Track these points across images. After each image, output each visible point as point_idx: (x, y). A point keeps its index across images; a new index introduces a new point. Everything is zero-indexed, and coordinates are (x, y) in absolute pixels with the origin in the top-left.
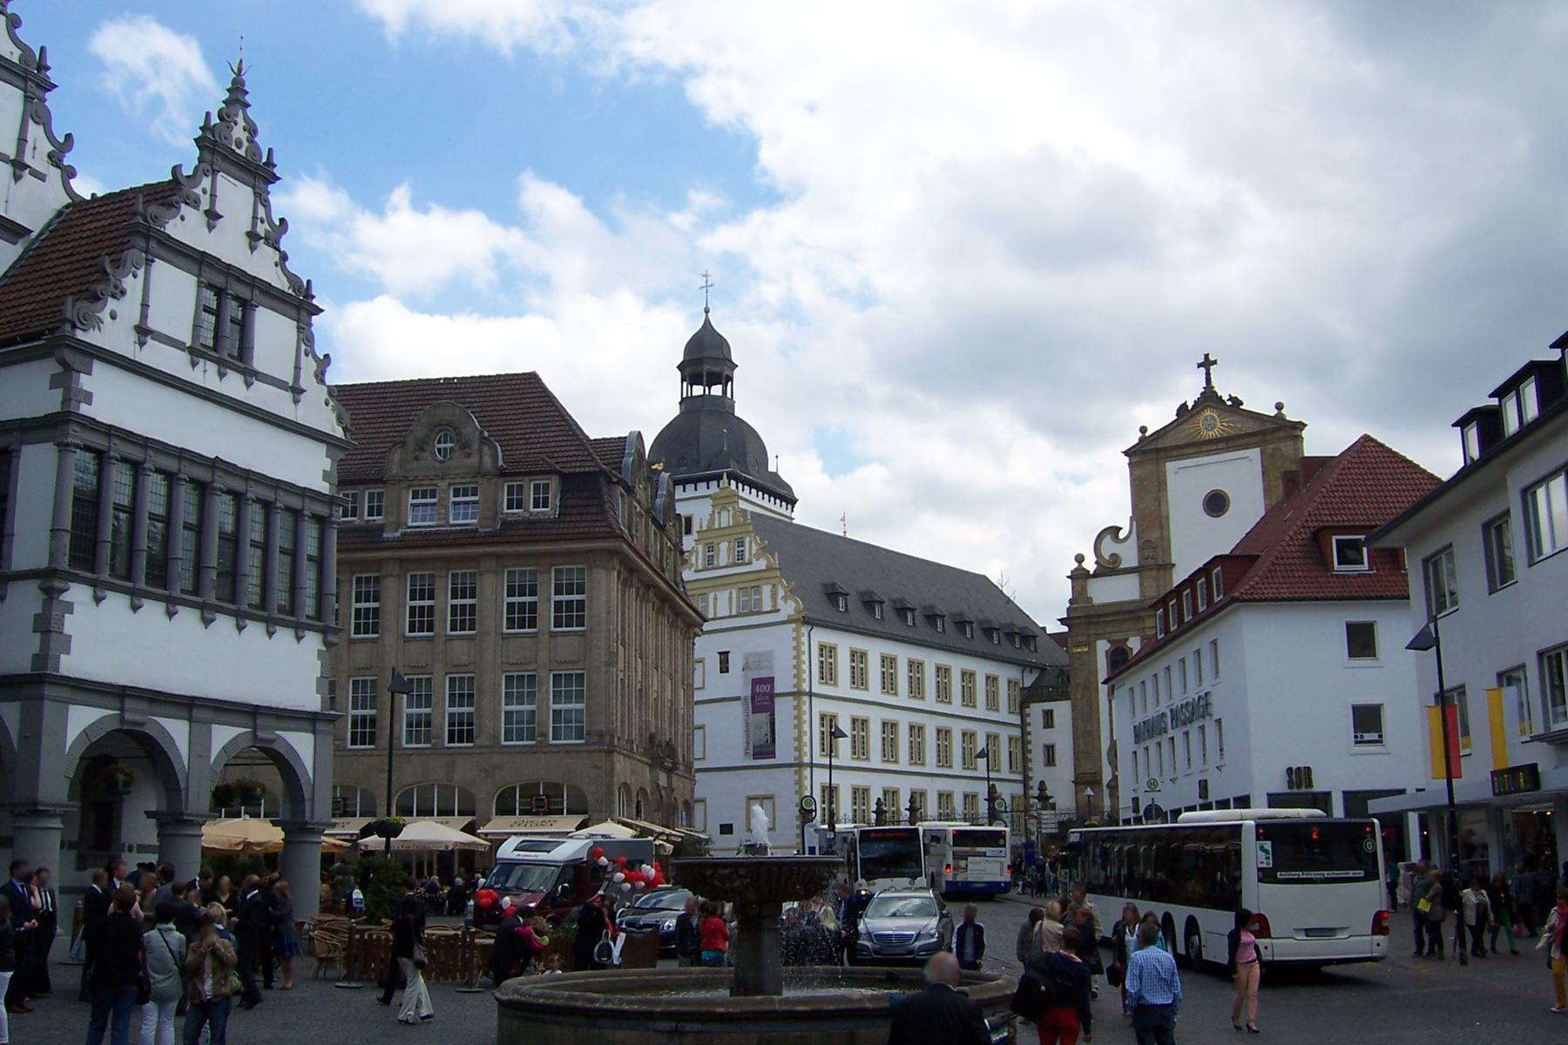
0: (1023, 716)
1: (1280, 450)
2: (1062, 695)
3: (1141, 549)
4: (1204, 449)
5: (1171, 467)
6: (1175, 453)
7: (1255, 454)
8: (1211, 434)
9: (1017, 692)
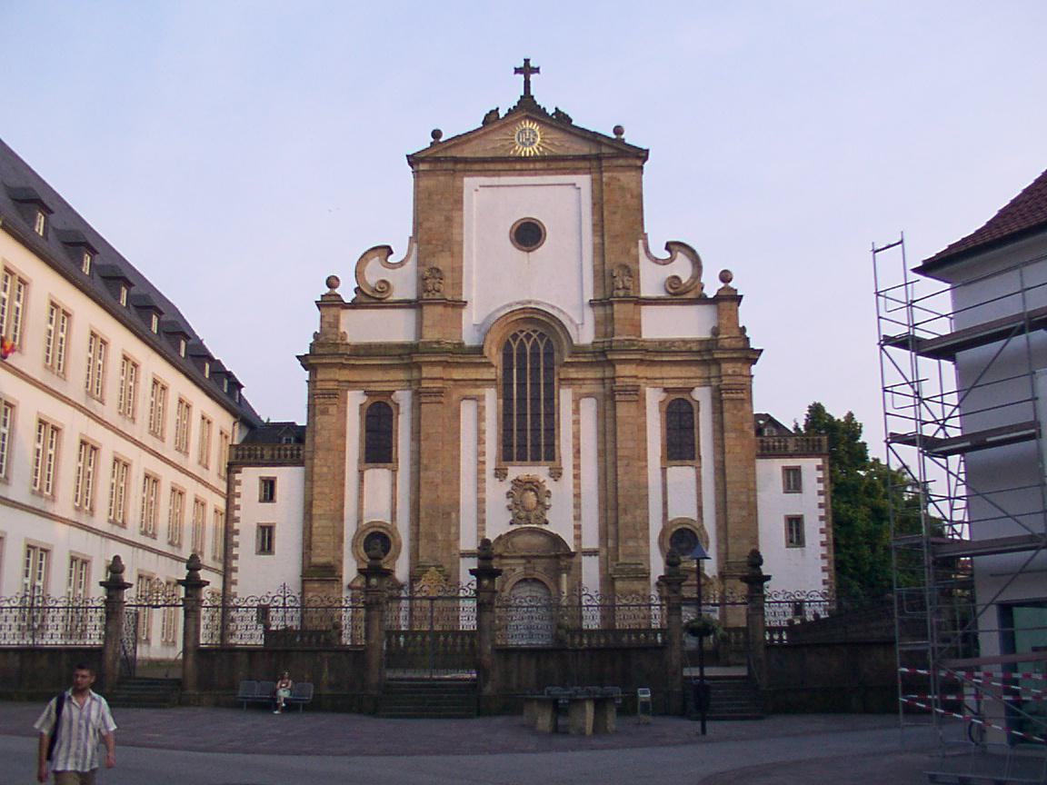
0: (231, 483)
1: (619, 180)
2: (296, 461)
3: (422, 279)
4: (518, 167)
5: (470, 183)
6: (477, 167)
7: (584, 181)
8: (529, 151)
9: (227, 449)
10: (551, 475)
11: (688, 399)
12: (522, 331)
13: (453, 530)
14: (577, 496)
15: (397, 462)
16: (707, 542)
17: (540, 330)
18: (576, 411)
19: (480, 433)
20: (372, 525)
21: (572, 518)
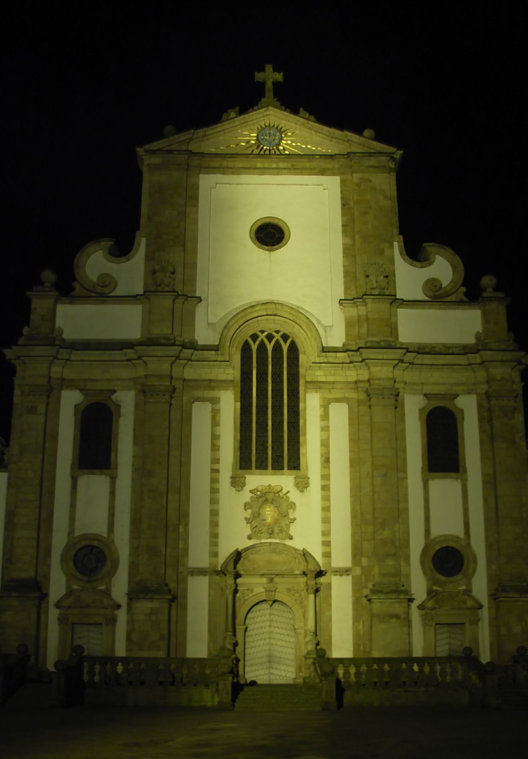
1: (371, 181)
10: (297, 485)
11: (451, 408)
12: (262, 332)
13: (181, 544)
14: (326, 509)
15: (116, 468)
16: (475, 561)
17: (283, 331)
18: (325, 416)
19: (215, 437)
20: (85, 537)
21: (320, 534)
